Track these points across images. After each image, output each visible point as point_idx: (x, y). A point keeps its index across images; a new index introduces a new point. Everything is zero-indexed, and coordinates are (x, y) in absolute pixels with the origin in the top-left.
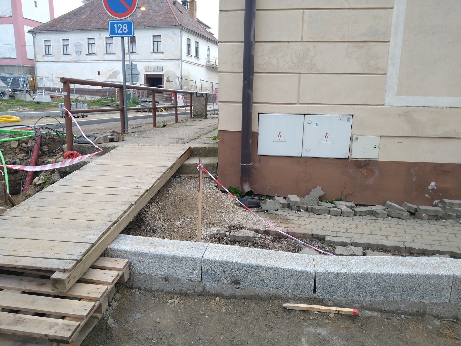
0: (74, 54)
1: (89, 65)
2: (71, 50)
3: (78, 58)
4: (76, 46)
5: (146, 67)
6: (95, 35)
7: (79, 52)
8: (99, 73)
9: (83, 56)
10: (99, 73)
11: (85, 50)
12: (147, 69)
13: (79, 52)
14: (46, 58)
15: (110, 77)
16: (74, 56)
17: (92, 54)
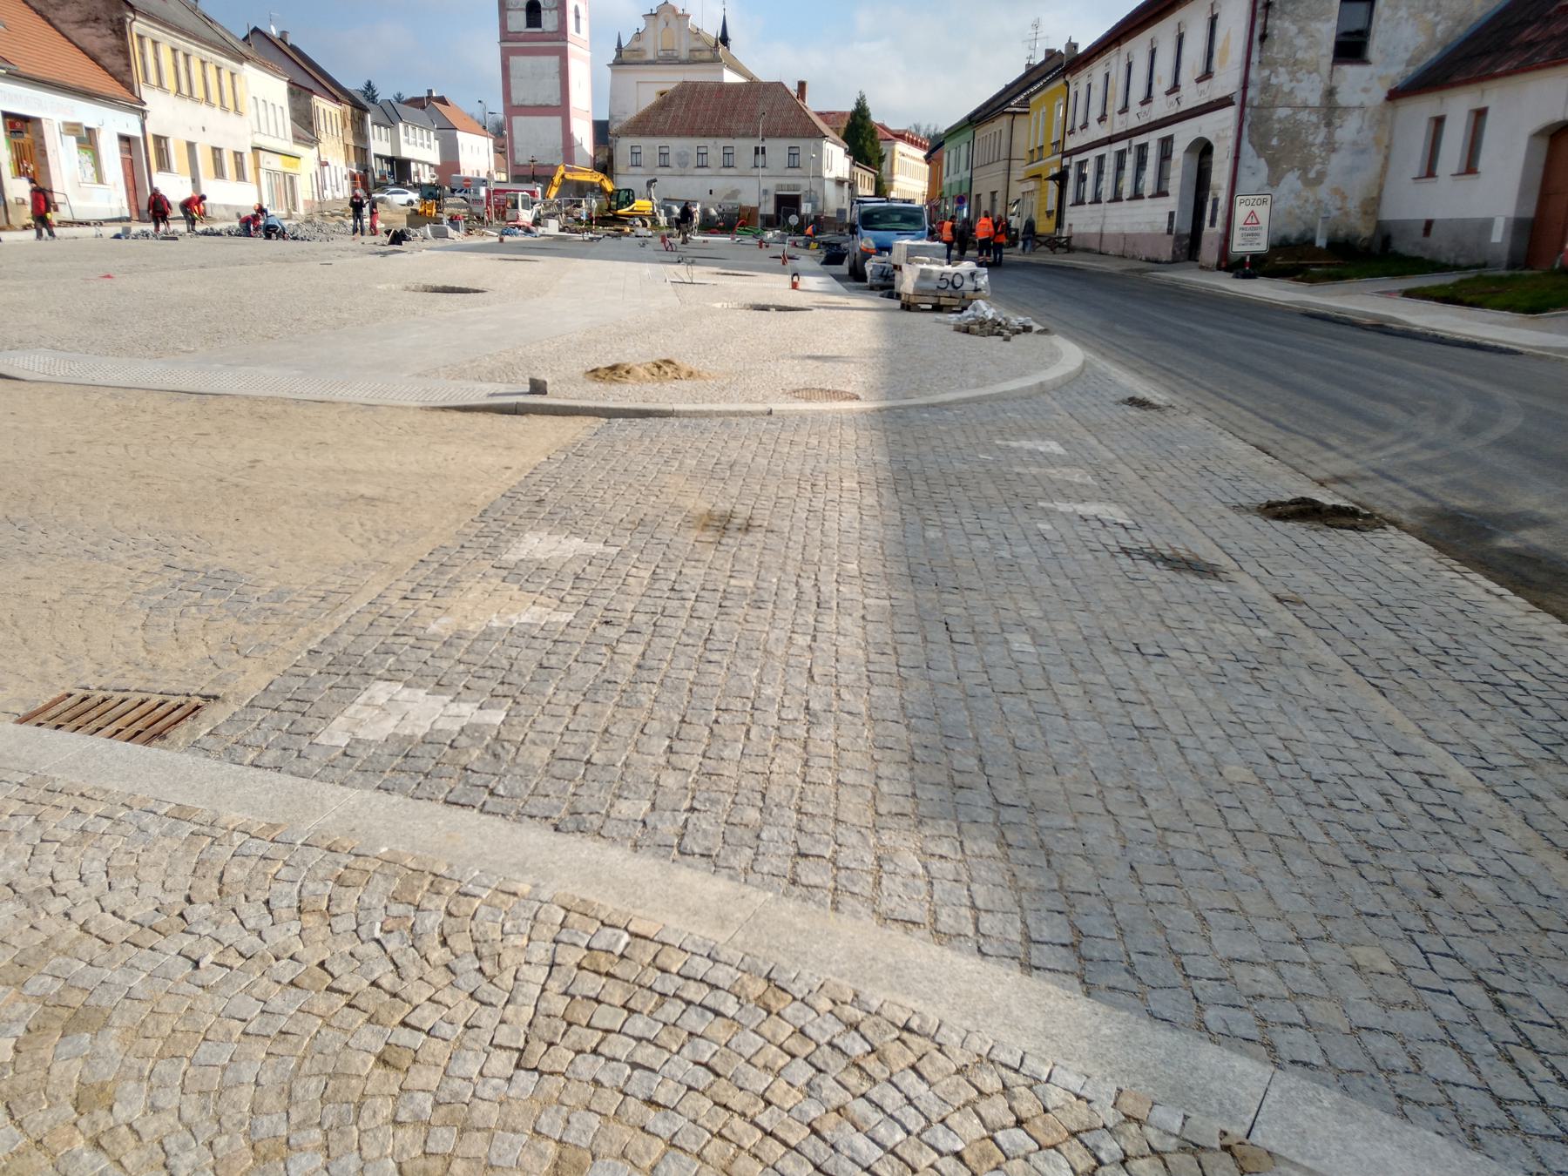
0: (676, 166)
1: (697, 181)
2: (672, 160)
3: (683, 171)
4: (679, 155)
5: (778, 185)
6: (709, 142)
7: (684, 165)
8: (711, 192)
9: (690, 169)
10: (711, 192)
11: (693, 161)
12: (780, 187)
13: (684, 165)
14: (633, 170)
15: (727, 197)
16: (676, 168)
17: (702, 167)
